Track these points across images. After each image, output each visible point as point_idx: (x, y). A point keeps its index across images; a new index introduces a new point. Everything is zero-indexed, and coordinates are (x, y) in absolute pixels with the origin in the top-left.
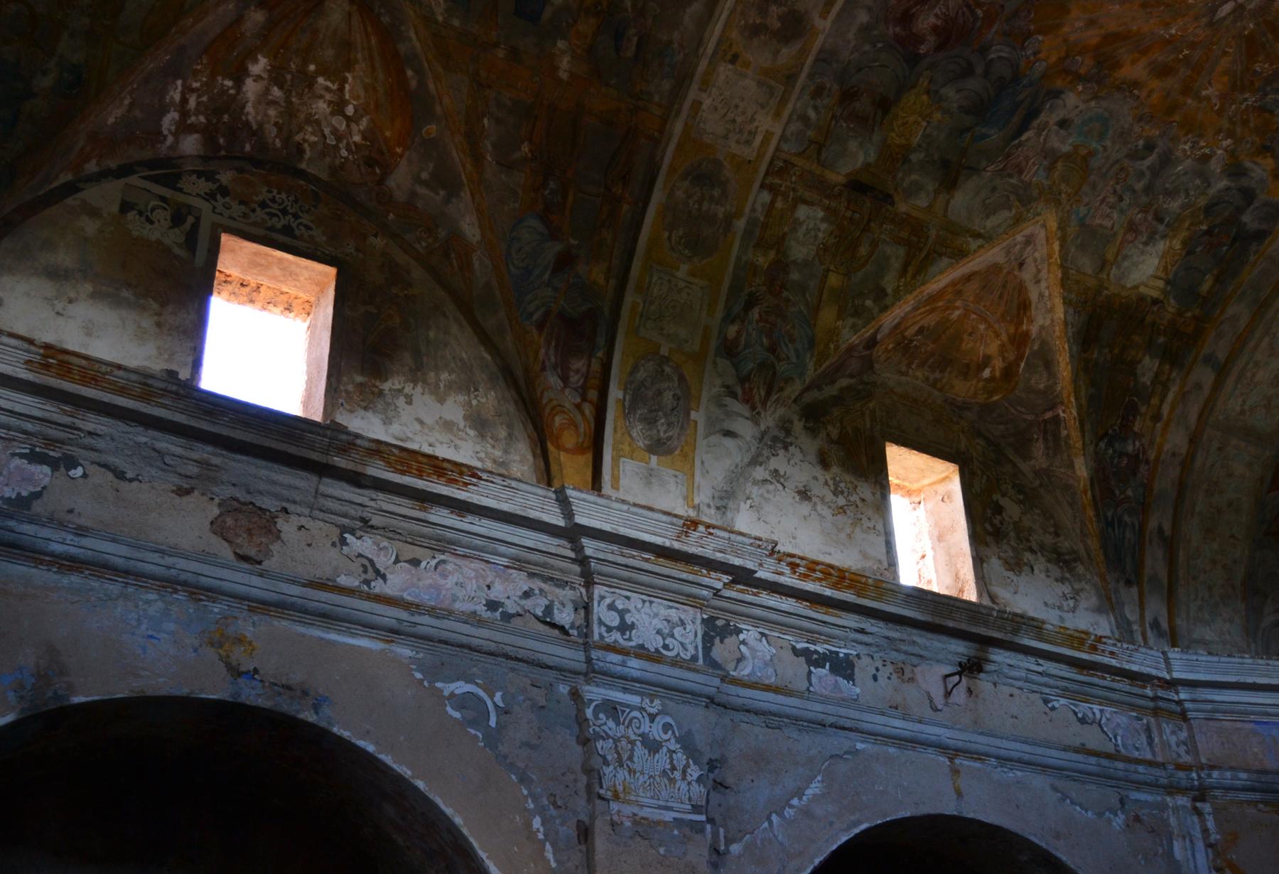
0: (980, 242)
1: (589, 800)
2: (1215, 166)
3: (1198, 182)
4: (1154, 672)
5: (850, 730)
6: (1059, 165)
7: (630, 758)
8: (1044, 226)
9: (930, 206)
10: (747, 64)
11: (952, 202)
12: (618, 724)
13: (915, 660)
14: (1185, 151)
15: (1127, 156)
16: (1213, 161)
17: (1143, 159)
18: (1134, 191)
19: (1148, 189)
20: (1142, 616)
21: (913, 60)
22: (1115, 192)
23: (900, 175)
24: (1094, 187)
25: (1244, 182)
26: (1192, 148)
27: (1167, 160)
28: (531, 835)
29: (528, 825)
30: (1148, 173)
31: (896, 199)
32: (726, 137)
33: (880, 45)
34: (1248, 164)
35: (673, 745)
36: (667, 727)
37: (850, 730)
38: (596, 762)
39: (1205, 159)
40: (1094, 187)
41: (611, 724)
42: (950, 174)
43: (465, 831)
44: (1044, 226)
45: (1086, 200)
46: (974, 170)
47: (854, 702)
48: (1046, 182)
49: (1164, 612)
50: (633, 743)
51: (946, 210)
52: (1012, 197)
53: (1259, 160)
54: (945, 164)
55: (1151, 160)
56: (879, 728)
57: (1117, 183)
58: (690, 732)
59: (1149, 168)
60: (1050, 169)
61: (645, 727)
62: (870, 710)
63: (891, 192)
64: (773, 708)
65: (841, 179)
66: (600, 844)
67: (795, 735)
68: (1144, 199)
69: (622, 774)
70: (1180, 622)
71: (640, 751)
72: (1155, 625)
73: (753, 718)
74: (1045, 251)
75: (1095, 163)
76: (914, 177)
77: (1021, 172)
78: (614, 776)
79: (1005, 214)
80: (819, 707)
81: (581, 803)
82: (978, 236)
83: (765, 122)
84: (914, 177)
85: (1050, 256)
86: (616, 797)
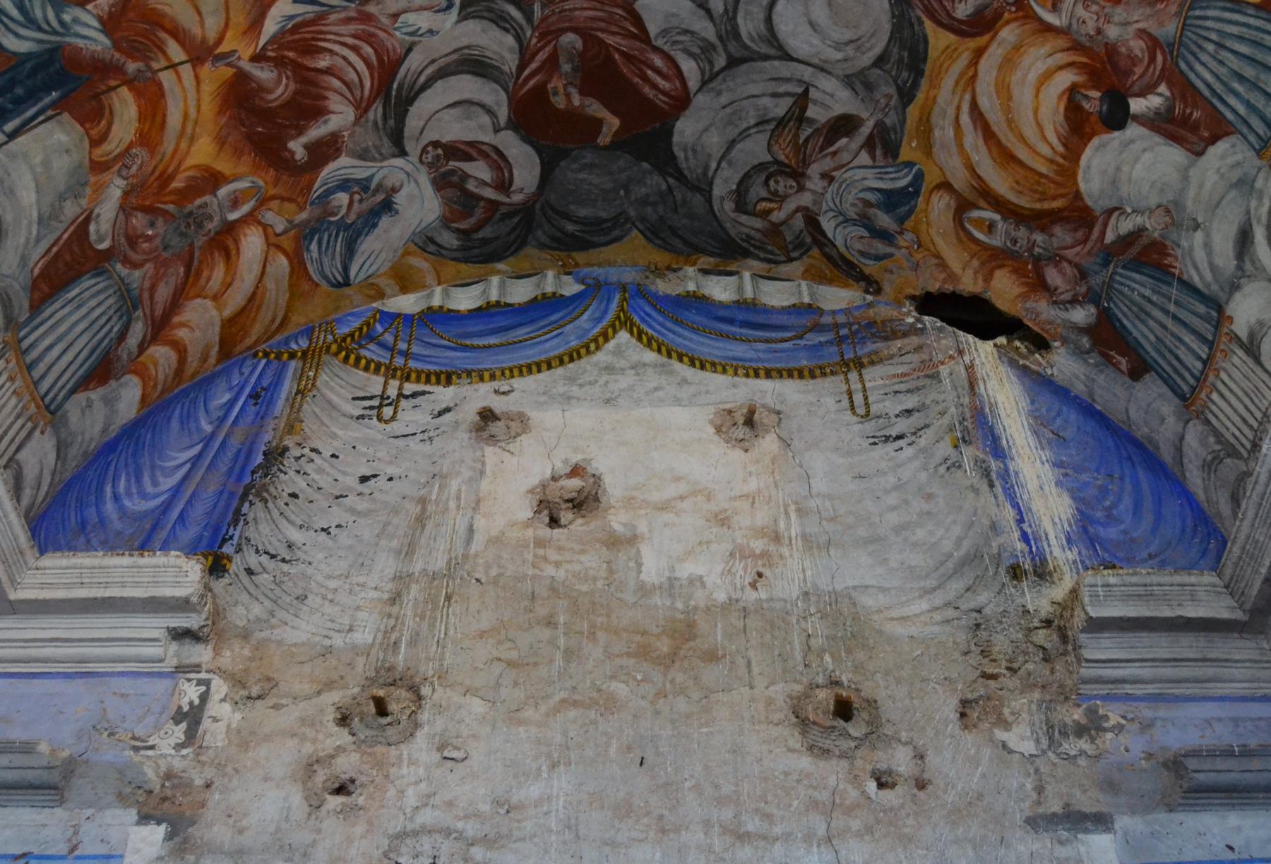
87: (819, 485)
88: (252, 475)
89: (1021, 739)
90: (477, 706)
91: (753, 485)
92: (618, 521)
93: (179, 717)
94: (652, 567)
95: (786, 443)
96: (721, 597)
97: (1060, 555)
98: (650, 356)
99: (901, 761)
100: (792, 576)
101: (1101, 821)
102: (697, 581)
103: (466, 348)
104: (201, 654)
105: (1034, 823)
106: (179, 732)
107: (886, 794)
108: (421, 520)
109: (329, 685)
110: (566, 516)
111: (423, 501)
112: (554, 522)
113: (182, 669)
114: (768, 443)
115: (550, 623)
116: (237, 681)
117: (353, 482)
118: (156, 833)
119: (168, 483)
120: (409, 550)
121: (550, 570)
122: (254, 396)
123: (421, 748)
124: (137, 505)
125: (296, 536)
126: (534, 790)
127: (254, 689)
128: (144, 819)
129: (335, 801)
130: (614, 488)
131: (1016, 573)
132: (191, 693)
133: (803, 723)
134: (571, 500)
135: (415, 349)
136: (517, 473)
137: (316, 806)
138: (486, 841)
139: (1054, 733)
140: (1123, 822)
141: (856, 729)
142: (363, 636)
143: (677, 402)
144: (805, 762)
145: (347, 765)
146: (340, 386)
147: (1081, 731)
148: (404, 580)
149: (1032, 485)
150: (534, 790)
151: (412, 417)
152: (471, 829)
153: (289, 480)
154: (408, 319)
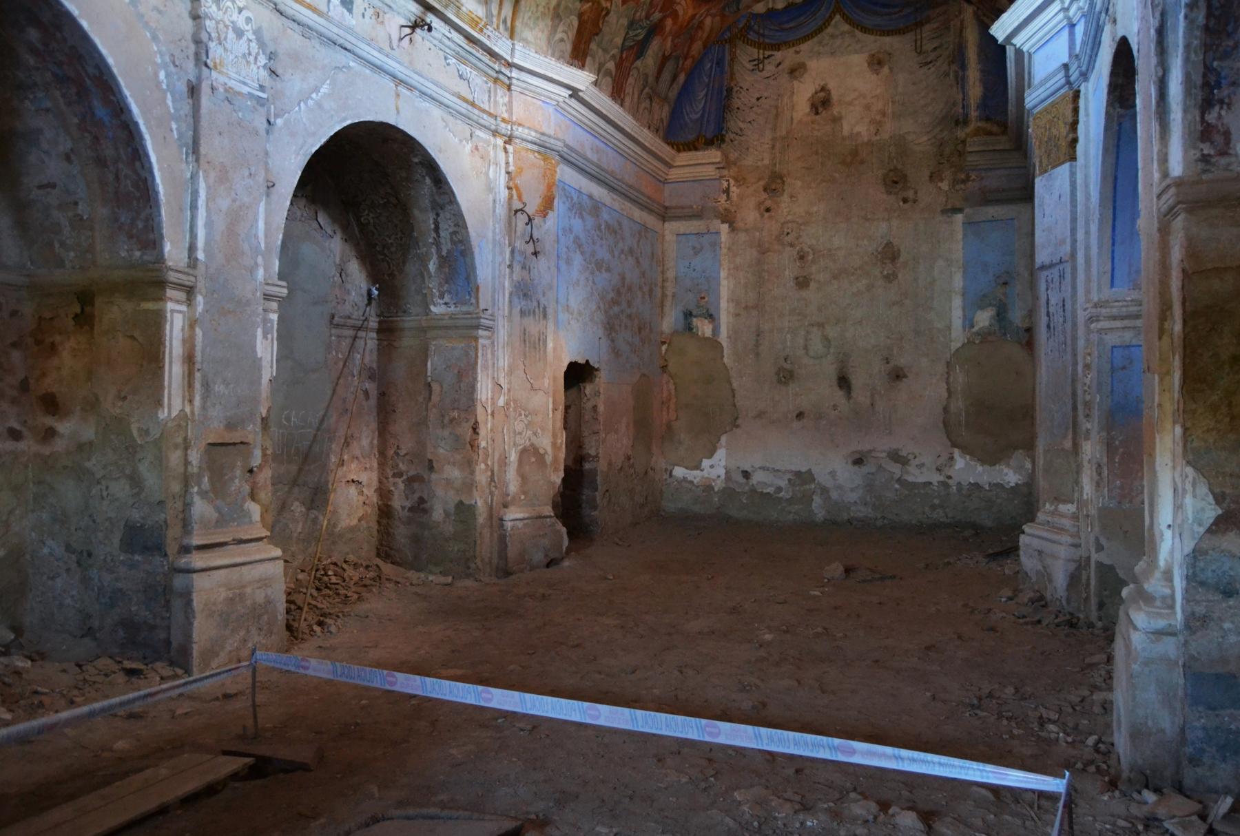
1: (196, 65)
4: (505, 56)
5: (349, 51)
7: (225, 39)
12: (219, 9)
13: (387, 9)
20: (499, 13)
28: (158, 84)
29: (156, 75)
35: (252, 37)
36: (248, 20)
37: (349, 51)
38: (204, 36)
41: (214, 8)
43: (115, 71)
47: (349, 30)
49: (510, 14)
50: (227, 26)
56: (364, 54)
58: (260, 28)
61: (235, 17)
62: (362, 40)
64: (311, 23)
66: (205, 100)
67: (317, 46)
69: (220, 50)
70: (518, 24)
71: (231, 35)
72: (505, 22)
73: (295, 26)
78: (215, 51)
80: (335, 30)
81: (190, 65)
86: (215, 67)
87: (900, 90)
88: (724, 100)
89: (945, 186)
90: (799, 183)
91: (879, 91)
92: (835, 111)
93: (724, 192)
94: (846, 132)
95: (891, 69)
96: (866, 139)
97: (974, 114)
98: (846, 27)
99: (910, 194)
100: (889, 128)
101: (960, 210)
102: (859, 133)
103: (783, 30)
104: (725, 172)
105: (944, 212)
106: (724, 197)
107: (906, 206)
108: (777, 116)
109: (760, 179)
110: (820, 110)
111: (777, 107)
112: (817, 113)
113: (722, 177)
114: (886, 70)
115: (817, 153)
116: (736, 180)
117: (754, 100)
118: (726, 226)
119: (701, 106)
120: (774, 129)
121: (816, 133)
122: (718, 63)
123: (785, 197)
124: (695, 116)
125: (742, 125)
126: (815, 209)
127: (740, 181)
128: (723, 222)
129: (767, 215)
130: (835, 96)
131: (957, 123)
132: (725, 184)
133: (885, 184)
134: (821, 103)
135: (766, 33)
136: (805, 91)
137: (762, 216)
138: (803, 224)
139: (955, 182)
140: (967, 210)
141: (899, 186)
142: (766, 162)
143: (856, 52)
144: (885, 196)
145: (768, 203)
146: (746, 54)
147: (963, 182)
148: (774, 139)
149: (971, 83)
150: (815, 209)
151: (770, 68)
152: (800, 221)
153: (736, 102)
154: (760, 15)
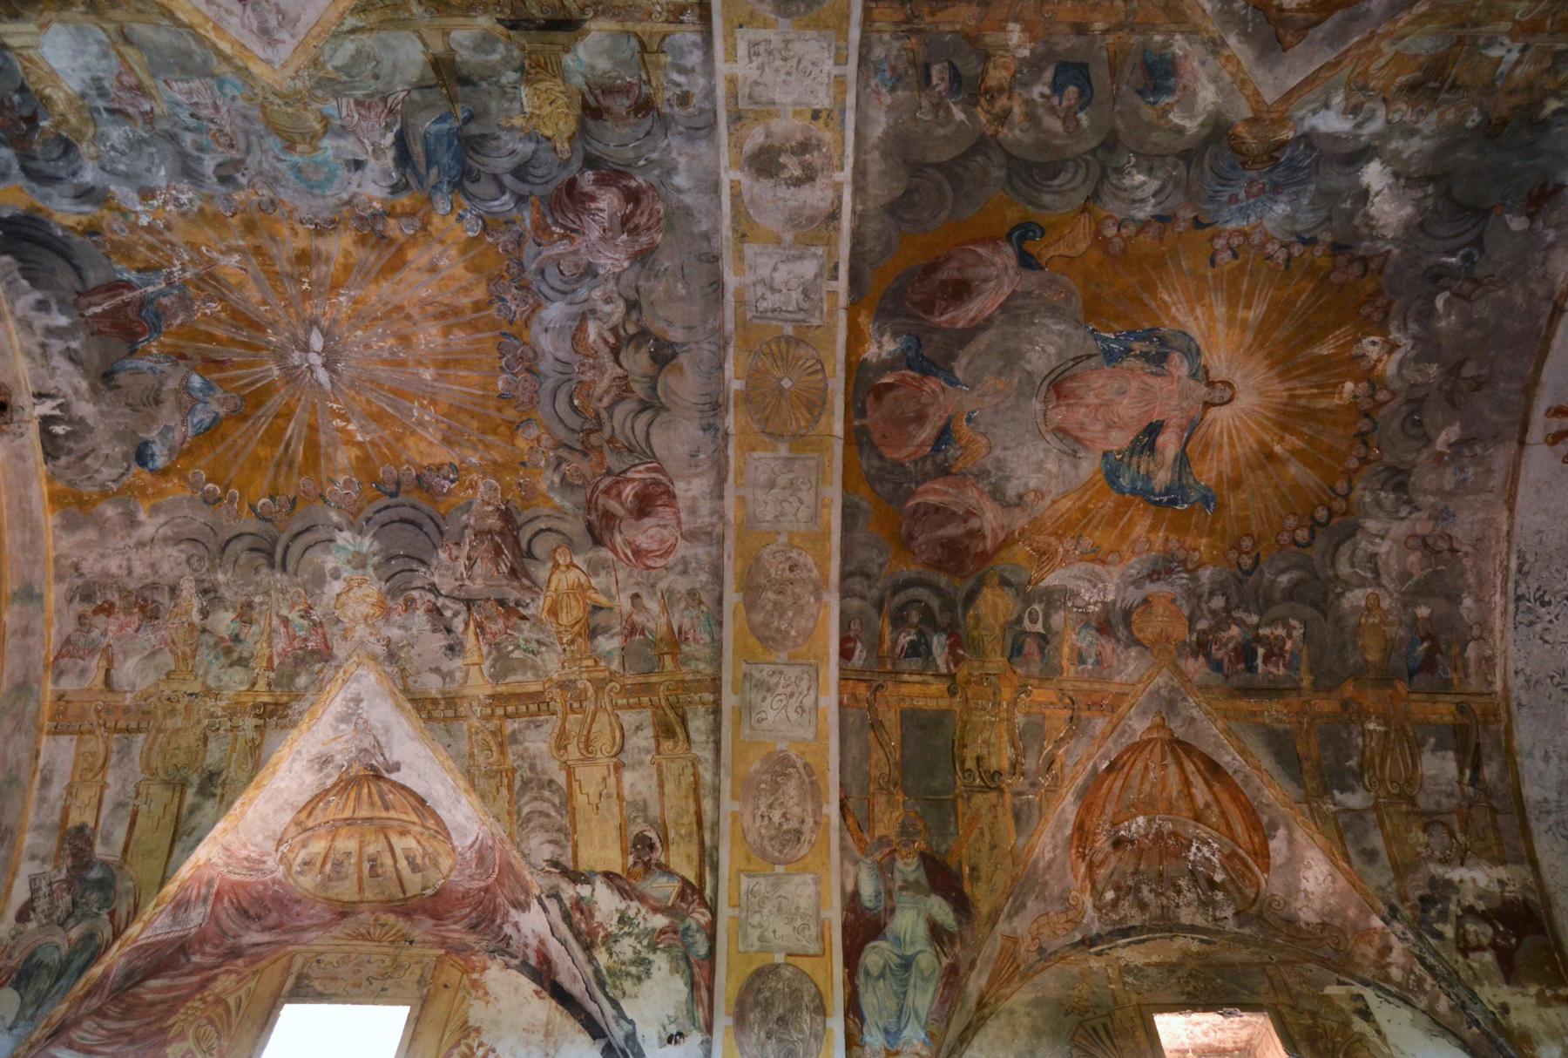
0: (346, 27)
2: (124, 193)
3: (122, 167)
6: (318, 127)
8: (268, 62)
9: (446, 34)
10: (797, 114)
11: (420, 46)
14: (182, 192)
15: (242, 161)
16: (136, 197)
17: (219, 166)
18: (187, 129)
19: (173, 138)
21: (590, 162)
22: (212, 121)
23: (516, 53)
24: (245, 117)
25: (66, 188)
26: (177, 199)
27: (188, 170)
30: (196, 153)
31: (500, 28)
32: (787, 42)
33: (642, 162)
34: (87, 208)
39: (147, 194)
40: (245, 117)
42: (446, 73)
44: (268, 62)
45: (240, 102)
46: (421, 86)
48: (315, 106)
51: (421, 38)
52: (344, 78)
53: (84, 219)
54: (465, 81)
55: (209, 164)
57: (220, 131)
59: (200, 159)
60: (325, 120)
63: (512, 33)
65: (591, 25)
68: (164, 125)
74: (232, 32)
75: (274, 143)
76: (496, 57)
77: (358, 103)
79: (341, 58)
82: (353, 31)
83: (744, 69)
84: (496, 57)
85: (216, 28)
